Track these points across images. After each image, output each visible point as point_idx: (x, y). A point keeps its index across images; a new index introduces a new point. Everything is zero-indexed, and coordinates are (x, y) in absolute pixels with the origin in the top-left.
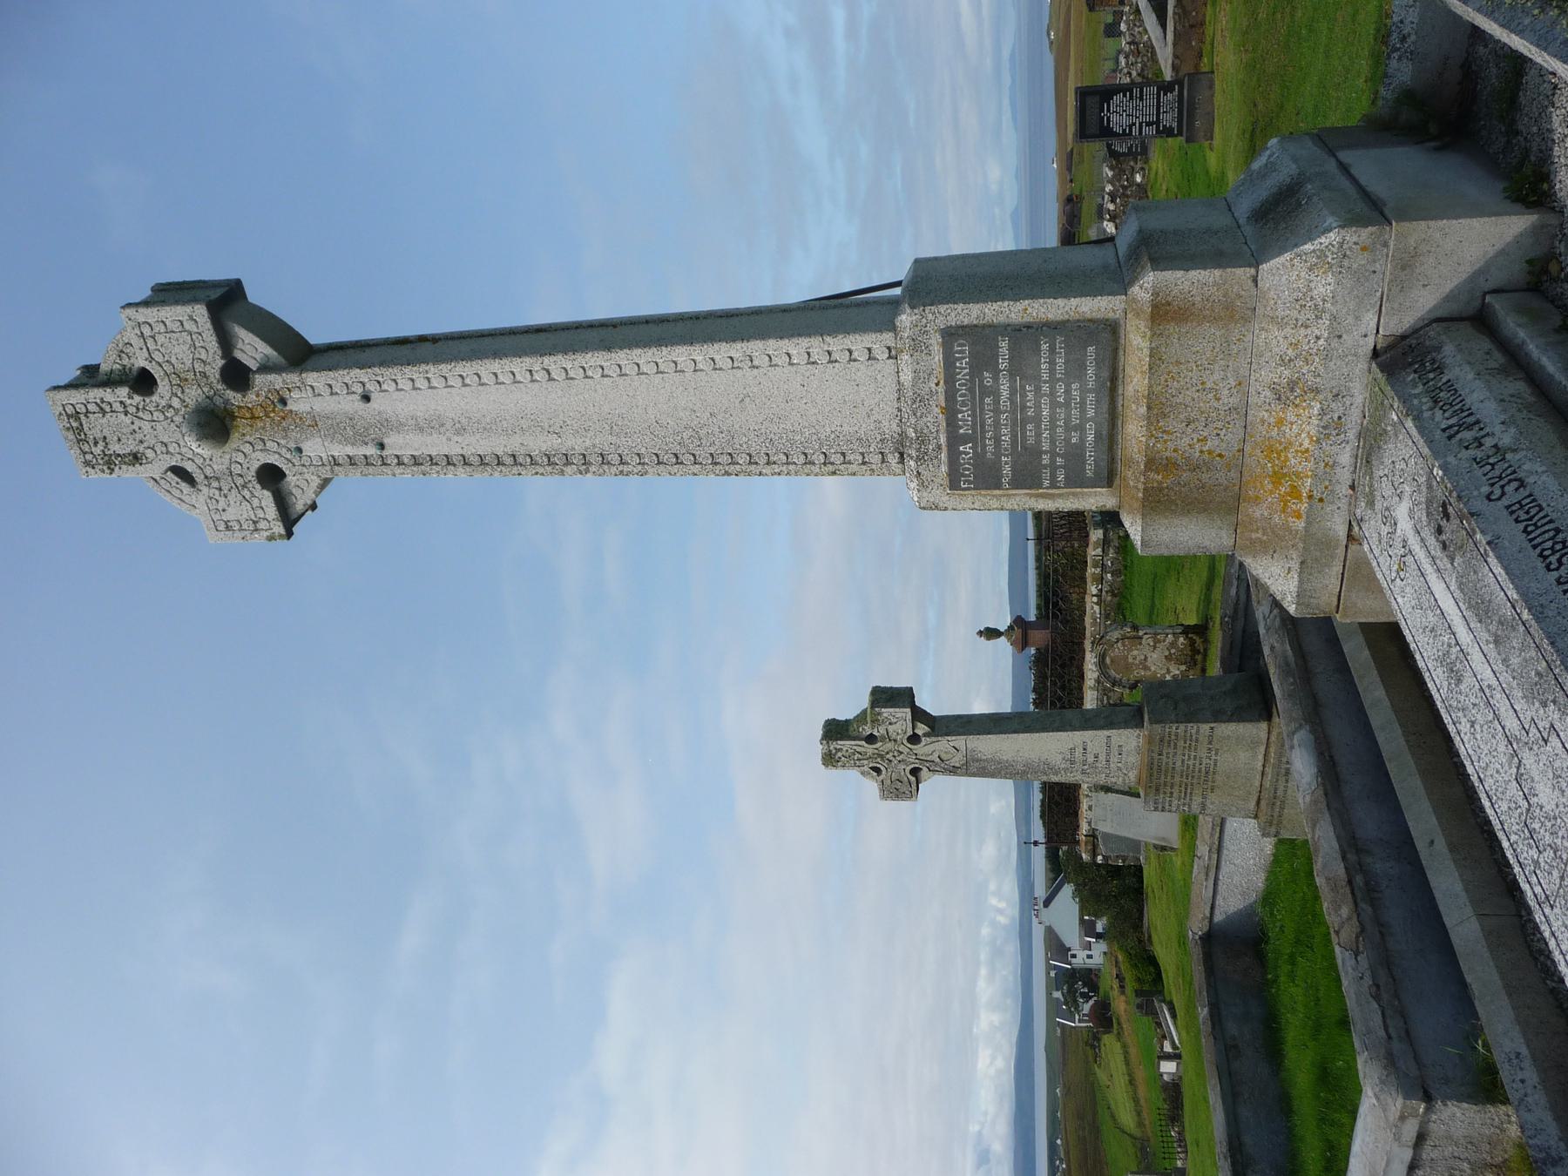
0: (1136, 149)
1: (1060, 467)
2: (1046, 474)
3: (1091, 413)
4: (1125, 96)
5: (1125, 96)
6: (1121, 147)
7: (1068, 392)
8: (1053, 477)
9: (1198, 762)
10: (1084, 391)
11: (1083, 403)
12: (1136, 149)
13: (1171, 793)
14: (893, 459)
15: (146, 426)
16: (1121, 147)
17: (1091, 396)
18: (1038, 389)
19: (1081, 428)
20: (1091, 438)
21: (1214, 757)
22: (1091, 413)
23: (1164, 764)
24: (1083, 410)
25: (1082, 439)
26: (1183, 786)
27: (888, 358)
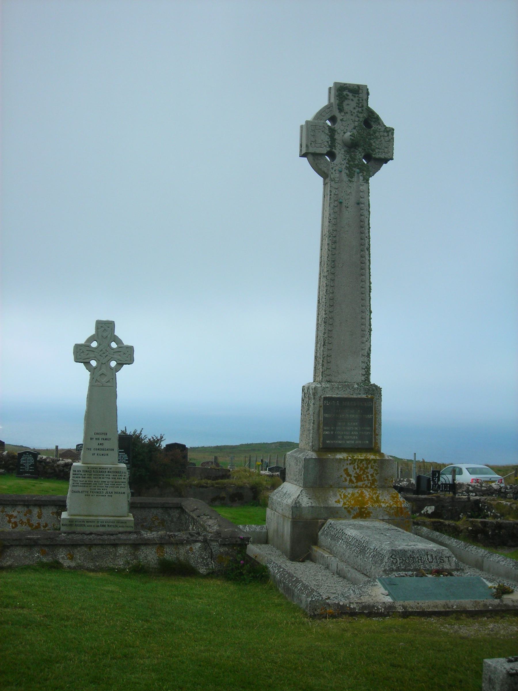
0: (22, 469)
1: (330, 433)
2: (328, 428)
3: (348, 442)
4: (127, 460)
5: (127, 460)
6: (24, 460)
7: (355, 435)
8: (327, 430)
9: (104, 488)
10: (355, 440)
11: (350, 439)
12: (22, 469)
13: (85, 477)
14: (327, 378)
15: (353, 118)
16: (24, 460)
17: (353, 442)
18: (356, 426)
19: (343, 439)
20: (340, 442)
21: (107, 495)
22: (348, 442)
23: (103, 474)
24: (348, 440)
25: (339, 439)
26: (89, 482)
27: (362, 380)
